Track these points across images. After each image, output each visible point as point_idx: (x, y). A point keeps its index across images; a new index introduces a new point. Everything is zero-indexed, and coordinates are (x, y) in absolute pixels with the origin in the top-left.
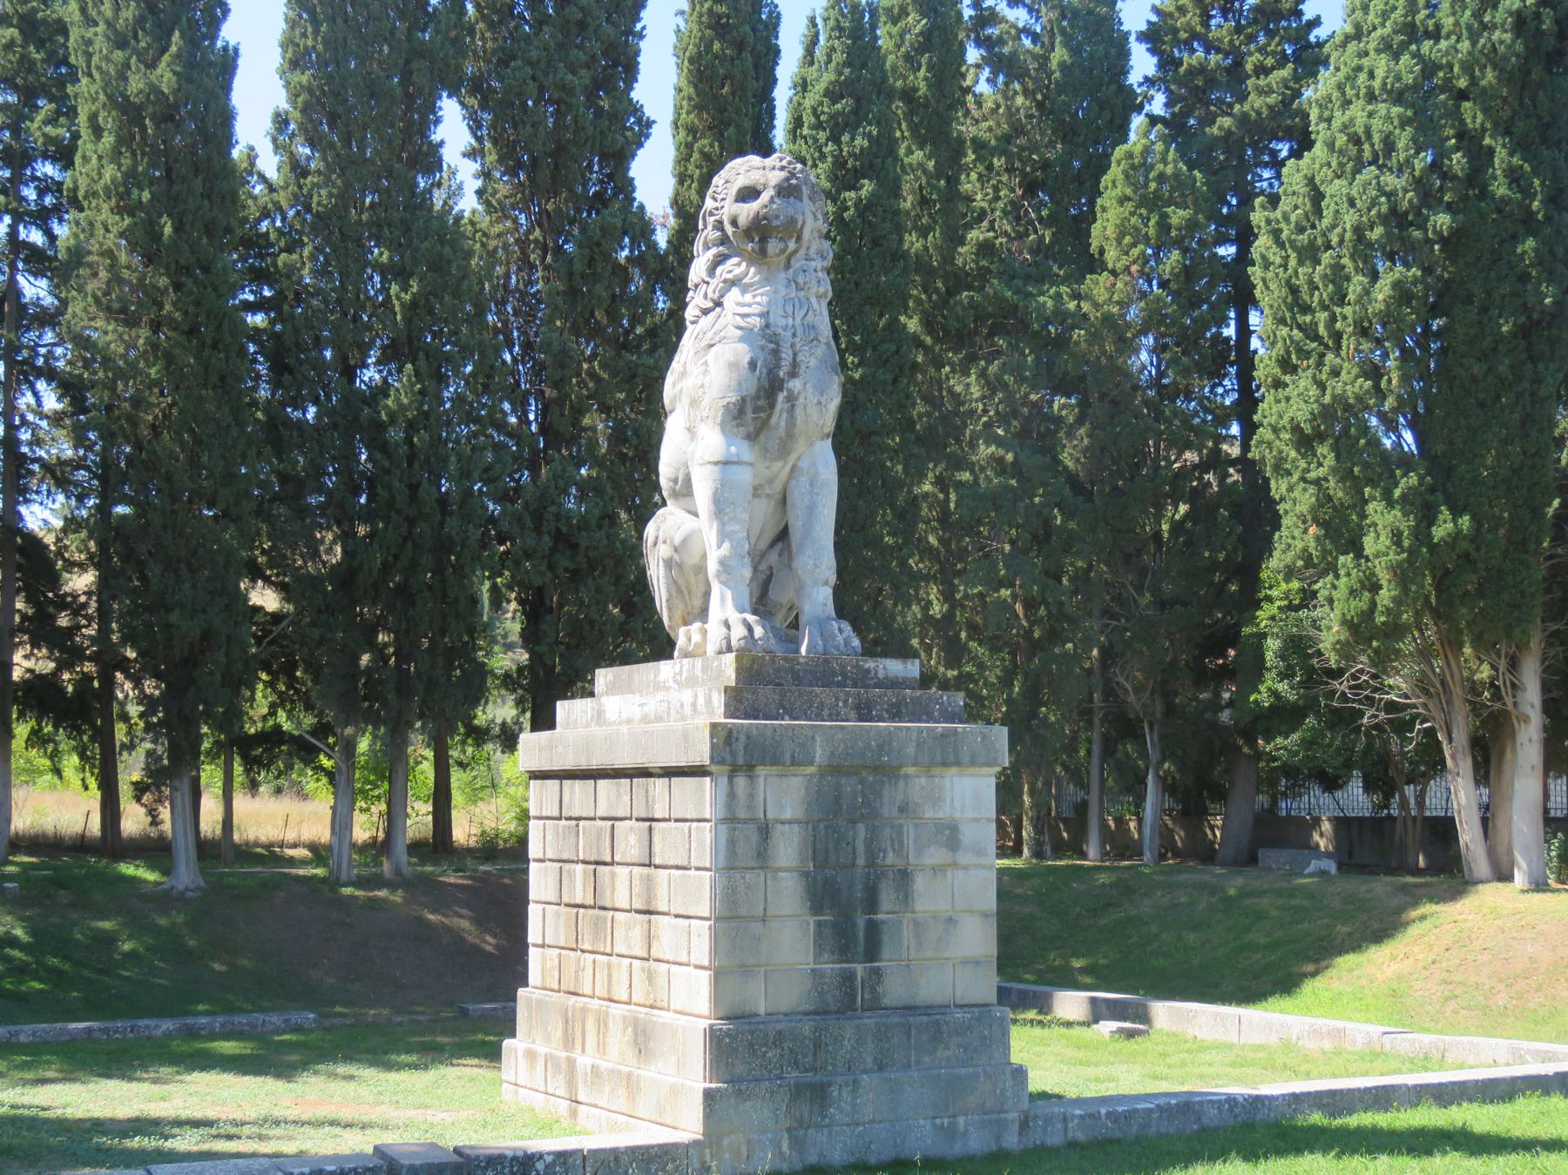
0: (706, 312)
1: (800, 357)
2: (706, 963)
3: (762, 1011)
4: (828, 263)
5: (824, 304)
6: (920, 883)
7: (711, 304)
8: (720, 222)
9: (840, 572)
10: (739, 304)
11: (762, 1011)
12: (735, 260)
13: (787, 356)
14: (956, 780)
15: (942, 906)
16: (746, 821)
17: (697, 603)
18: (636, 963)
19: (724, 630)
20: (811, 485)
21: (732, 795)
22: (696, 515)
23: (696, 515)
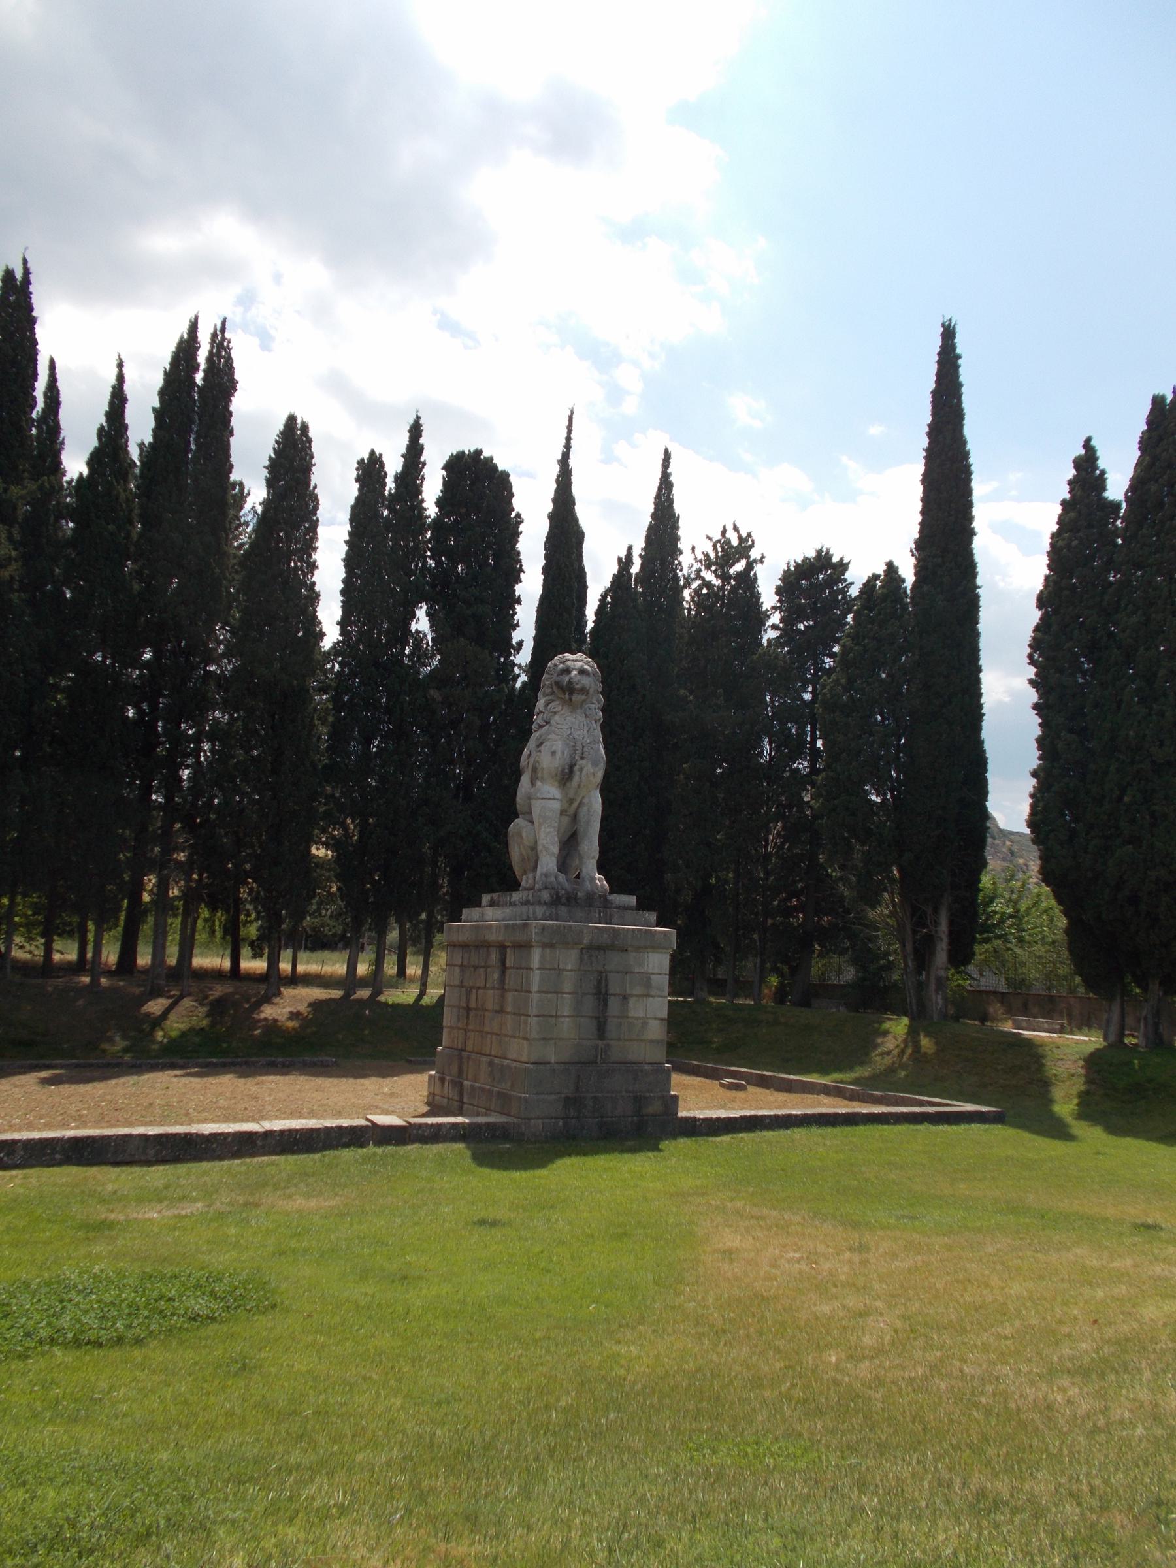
1: (585, 749)
3: (553, 1061)
4: (601, 705)
5: (599, 724)
6: (632, 1002)
9: (601, 852)
11: (553, 1061)
12: (557, 702)
13: (579, 748)
15: (641, 1014)
16: (550, 969)
17: (532, 864)
18: (494, 1037)
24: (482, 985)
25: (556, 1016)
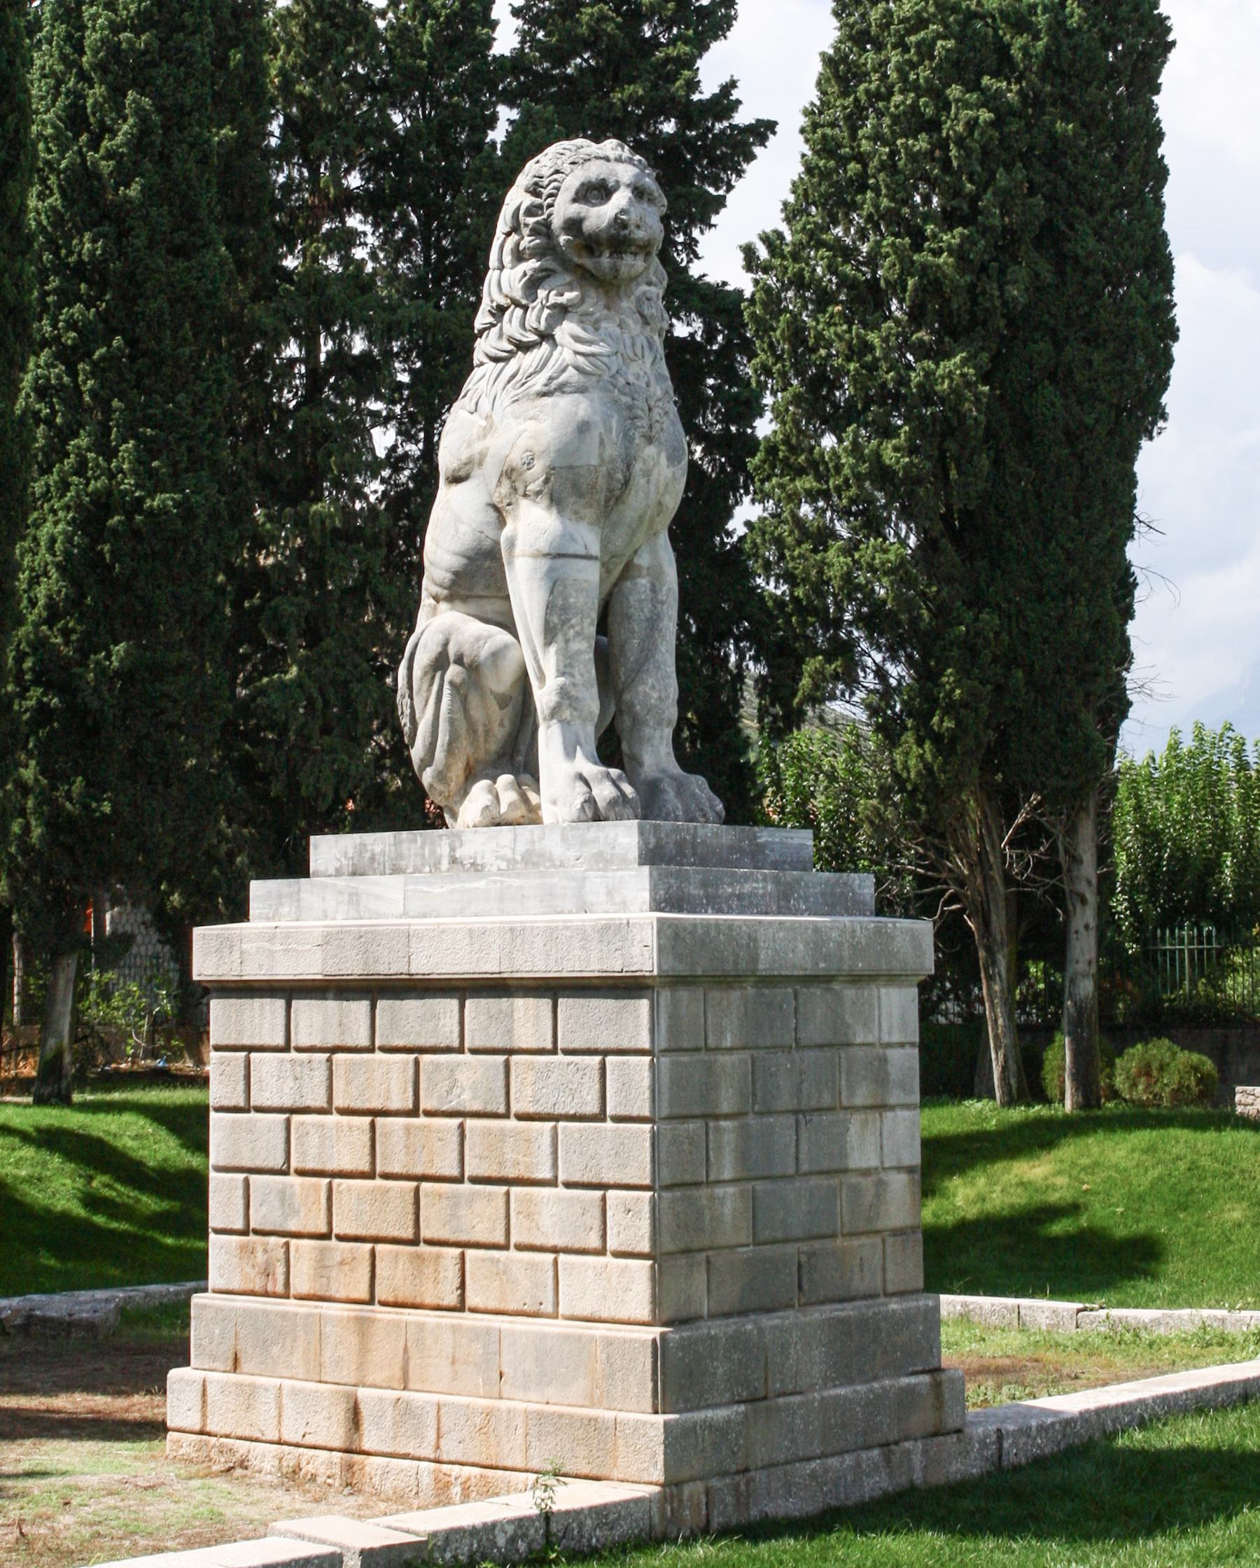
0: (524, 347)
2: (645, 1247)
7: (533, 337)
8: (547, 224)
10: (577, 339)
14: (883, 990)
19: (586, 789)
20: (654, 589)
21: (674, 1018)
22: (510, 627)
23: (510, 627)
24: (395, 1105)
25: (709, 1184)
